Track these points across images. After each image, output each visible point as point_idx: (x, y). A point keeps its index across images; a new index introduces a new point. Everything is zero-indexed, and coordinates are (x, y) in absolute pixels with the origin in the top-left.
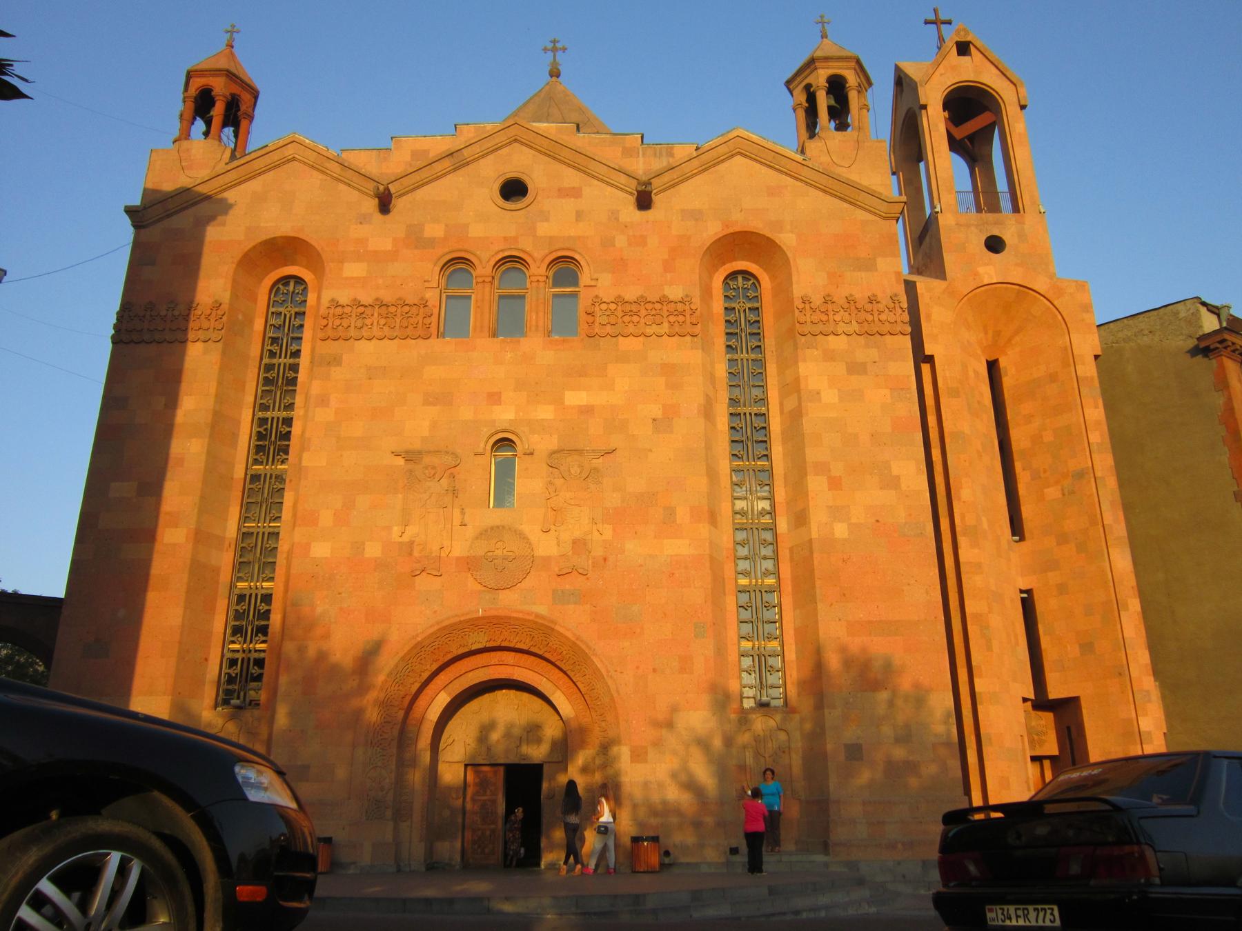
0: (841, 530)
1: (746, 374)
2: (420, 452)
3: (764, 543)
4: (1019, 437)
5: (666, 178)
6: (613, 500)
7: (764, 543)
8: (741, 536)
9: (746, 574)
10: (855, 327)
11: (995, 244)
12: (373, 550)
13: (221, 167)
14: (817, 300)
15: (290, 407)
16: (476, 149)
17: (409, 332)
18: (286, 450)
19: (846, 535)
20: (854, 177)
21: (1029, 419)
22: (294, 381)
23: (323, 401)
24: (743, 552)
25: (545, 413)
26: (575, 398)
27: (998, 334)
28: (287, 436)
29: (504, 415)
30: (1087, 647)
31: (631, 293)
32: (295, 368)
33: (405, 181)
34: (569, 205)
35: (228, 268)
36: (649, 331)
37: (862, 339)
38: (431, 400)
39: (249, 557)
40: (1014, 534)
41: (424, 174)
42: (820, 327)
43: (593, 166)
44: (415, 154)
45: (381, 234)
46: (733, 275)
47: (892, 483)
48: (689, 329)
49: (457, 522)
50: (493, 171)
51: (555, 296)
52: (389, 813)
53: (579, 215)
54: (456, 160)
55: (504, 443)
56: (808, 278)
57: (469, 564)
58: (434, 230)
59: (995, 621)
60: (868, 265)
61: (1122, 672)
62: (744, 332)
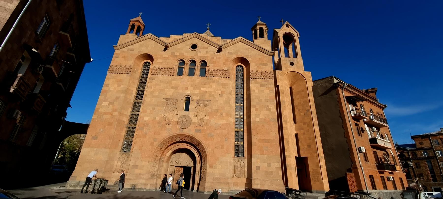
0: (257, 119)
1: (239, 86)
2: (169, 99)
3: (241, 121)
4: (296, 102)
5: (225, 46)
6: (209, 111)
7: (241, 121)
8: (236, 120)
9: (237, 128)
10: (263, 77)
11: (292, 64)
12: (157, 119)
13: (134, 39)
14: (255, 71)
15: (144, 88)
16: (187, 38)
17: (170, 74)
18: (142, 97)
19: (258, 120)
20: (264, 47)
21: (298, 99)
22: (145, 83)
23: (151, 87)
24: (237, 123)
25: (197, 92)
26: (203, 89)
27: (292, 82)
28: (143, 94)
29: (188, 92)
30: (309, 146)
31: (216, 68)
32: (146, 80)
33: (172, 44)
34: (205, 50)
35: (133, 59)
36: (220, 76)
37: (264, 80)
38: (173, 88)
39: (132, 119)
40: (294, 122)
41: (176, 42)
42: (256, 77)
43: (210, 43)
44: (174, 39)
45: (166, 54)
46: (238, 66)
47: (269, 110)
48: (228, 76)
49: (176, 114)
50: (190, 43)
51: (201, 68)
52: (155, 177)
53: (207, 52)
54: (183, 41)
55: (188, 98)
56: (253, 67)
57: (178, 123)
58: (177, 54)
59: (290, 140)
60: (266, 65)
61: (317, 152)
62: (239, 77)
